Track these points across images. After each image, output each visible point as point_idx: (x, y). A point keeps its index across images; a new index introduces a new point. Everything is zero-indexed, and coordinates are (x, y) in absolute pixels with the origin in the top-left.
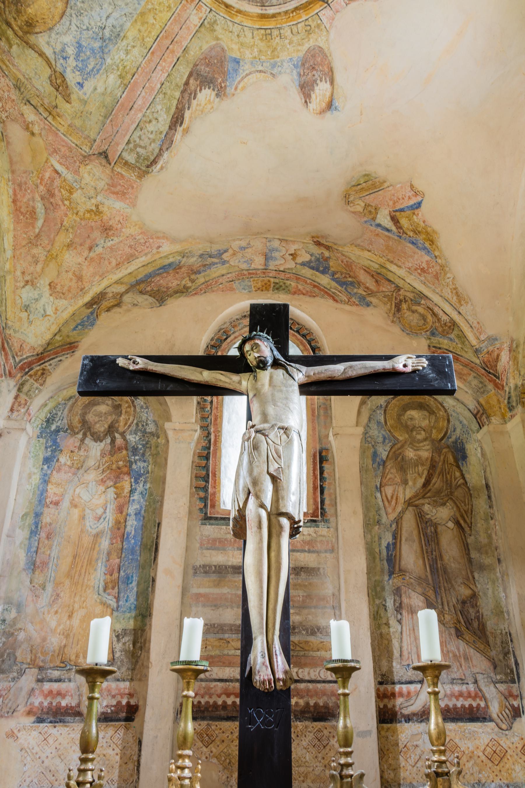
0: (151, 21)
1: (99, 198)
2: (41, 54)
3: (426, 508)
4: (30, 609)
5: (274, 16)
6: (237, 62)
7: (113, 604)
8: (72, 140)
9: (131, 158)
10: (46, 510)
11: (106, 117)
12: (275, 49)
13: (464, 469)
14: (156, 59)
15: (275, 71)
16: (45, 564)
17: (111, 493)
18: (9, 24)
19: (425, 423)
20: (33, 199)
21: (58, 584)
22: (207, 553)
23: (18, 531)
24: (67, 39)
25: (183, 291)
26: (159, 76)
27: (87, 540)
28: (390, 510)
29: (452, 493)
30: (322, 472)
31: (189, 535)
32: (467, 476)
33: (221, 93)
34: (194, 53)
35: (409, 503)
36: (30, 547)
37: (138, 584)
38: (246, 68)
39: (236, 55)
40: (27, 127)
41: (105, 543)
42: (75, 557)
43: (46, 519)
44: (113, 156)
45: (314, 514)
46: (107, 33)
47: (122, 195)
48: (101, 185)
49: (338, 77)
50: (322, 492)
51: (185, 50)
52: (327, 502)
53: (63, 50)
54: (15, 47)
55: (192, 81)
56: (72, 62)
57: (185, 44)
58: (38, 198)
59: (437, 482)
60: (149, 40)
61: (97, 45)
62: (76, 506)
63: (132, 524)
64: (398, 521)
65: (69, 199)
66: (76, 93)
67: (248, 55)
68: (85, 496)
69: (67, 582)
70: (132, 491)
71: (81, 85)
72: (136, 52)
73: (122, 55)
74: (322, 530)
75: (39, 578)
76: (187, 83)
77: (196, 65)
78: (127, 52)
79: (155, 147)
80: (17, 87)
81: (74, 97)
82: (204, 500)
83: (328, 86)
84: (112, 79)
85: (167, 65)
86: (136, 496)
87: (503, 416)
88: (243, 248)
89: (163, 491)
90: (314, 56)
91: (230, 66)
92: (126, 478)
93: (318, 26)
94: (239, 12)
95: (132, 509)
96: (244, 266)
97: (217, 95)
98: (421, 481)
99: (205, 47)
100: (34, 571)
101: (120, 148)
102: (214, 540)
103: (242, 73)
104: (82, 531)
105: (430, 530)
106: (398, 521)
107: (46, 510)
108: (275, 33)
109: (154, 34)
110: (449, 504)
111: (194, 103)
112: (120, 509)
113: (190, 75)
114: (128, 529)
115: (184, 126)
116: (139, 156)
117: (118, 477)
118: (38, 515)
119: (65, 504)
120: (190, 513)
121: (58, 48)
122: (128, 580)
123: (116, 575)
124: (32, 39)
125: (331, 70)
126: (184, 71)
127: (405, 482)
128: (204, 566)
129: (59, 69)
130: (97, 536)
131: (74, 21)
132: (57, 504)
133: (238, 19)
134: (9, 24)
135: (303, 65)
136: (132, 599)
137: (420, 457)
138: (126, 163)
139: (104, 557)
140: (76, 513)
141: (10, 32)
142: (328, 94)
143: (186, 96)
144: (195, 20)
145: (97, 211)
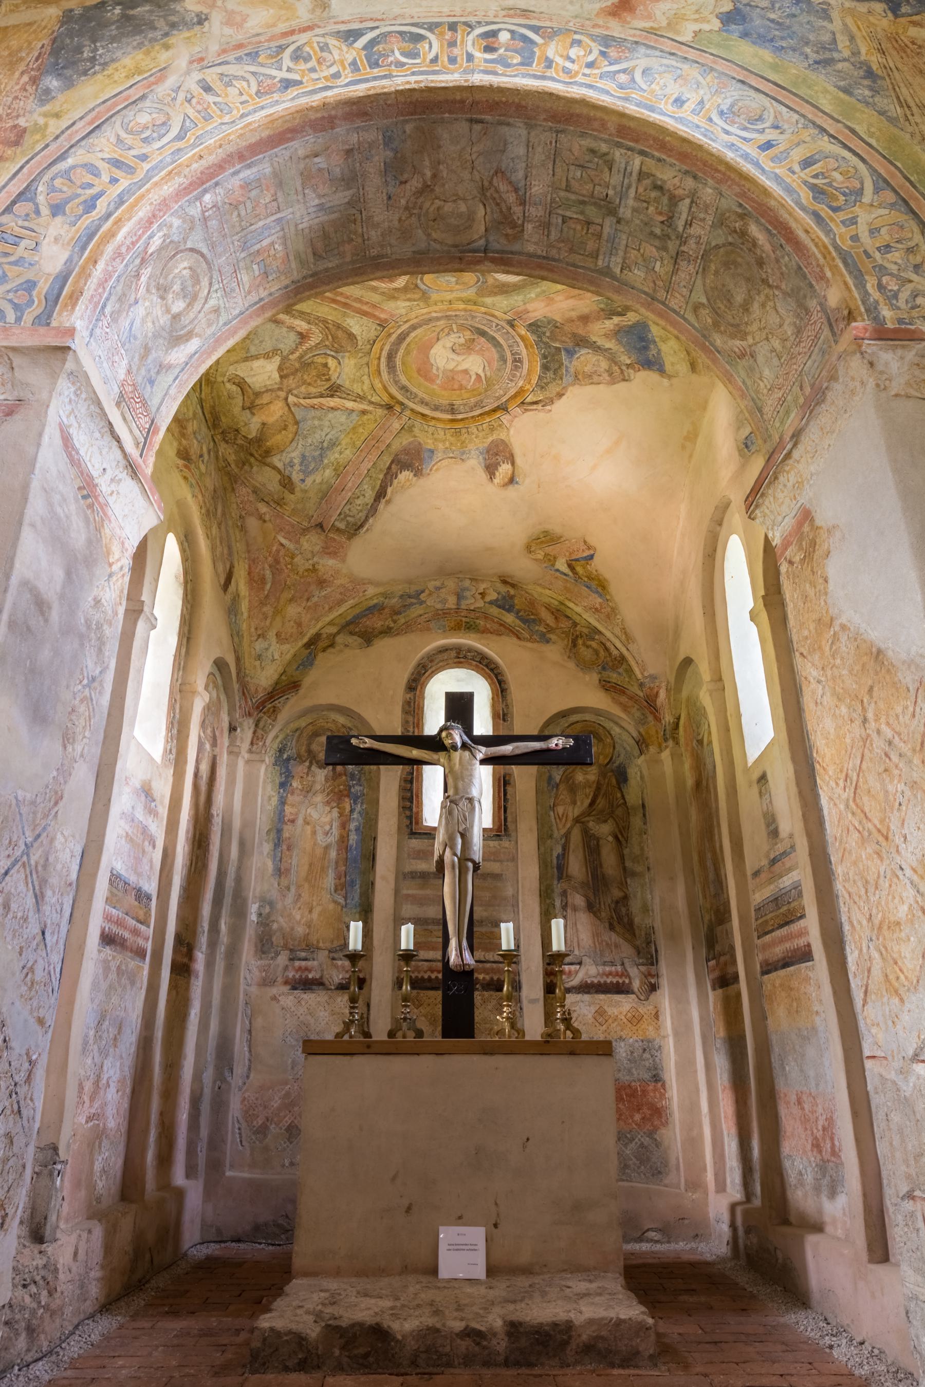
0: (361, 430)
1: (315, 559)
2: (275, 468)
3: (591, 824)
4: (279, 906)
5: (462, 420)
6: (432, 451)
7: (342, 901)
8: (294, 520)
9: (342, 525)
10: (285, 827)
11: (322, 499)
12: (463, 442)
13: (624, 791)
14: (364, 454)
15: (464, 457)
16: (288, 870)
18: (252, 455)
20: (264, 569)
21: (299, 887)
22: (413, 861)
23: (265, 844)
24: (293, 455)
26: (367, 465)
27: (319, 852)
28: (560, 826)
29: (613, 812)
30: (505, 794)
31: (399, 847)
32: (627, 797)
33: (418, 473)
34: (396, 446)
35: (577, 820)
36: (275, 856)
37: (361, 887)
38: (439, 455)
39: (431, 447)
40: (261, 518)
41: (333, 854)
42: (310, 865)
43: (286, 834)
45: (499, 830)
46: (325, 445)
47: (333, 554)
48: (317, 548)
49: (519, 460)
50: (505, 811)
51: (389, 446)
52: (509, 819)
53: (291, 461)
54: (255, 468)
55: (393, 466)
56: (297, 467)
57: (388, 442)
58: (267, 566)
59: (601, 803)
60: (358, 443)
61: (318, 453)
62: (308, 824)
63: (353, 838)
64: (567, 836)
65: (291, 564)
66: (299, 486)
67: (441, 446)
69: (306, 885)
71: (303, 481)
72: (348, 452)
73: (337, 455)
74: (505, 843)
75: (285, 882)
76: (389, 468)
77: (397, 455)
78: (341, 453)
80: (255, 492)
81: (297, 489)
83: (509, 466)
84: (328, 473)
85: (373, 457)
86: (355, 815)
87: (660, 745)
89: (377, 811)
90: (497, 446)
91: (426, 455)
92: (347, 800)
93: (500, 426)
94: (433, 418)
95: (353, 826)
97: (415, 475)
98: (587, 802)
99: (405, 442)
100: (280, 876)
101: (333, 519)
102: (419, 852)
103: (435, 459)
104: (315, 844)
105: (594, 842)
106: (567, 836)
107: (285, 827)
108: (464, 431)
109: (363, 438)
110: (610, 821)
111: (395, 482)
112: (343, 826)
113: (392, 462)
114: (351, 842)
115: (387, 498)
116: (348, 523)
117: (340, 799)
118: (279, 831)
119: (300, 821)
120: (399, 828)
121: (288, 460)
122: (352, 884)
123: (343, 880)
124: (268, 460)
125: (512, 456)
126: (387, 460)
127: (574, 803)
128: (411, 873)
129: (287, 473)
130: (327, 848)
131: (301, 442)
132: (293, 821)
133: (433, 423)
134: (252, 455)
135: (488, 452)
136: (357, 898)
137: (588, 781)
138: (338, 530)
139: (333, 864)
140: (308, 829)
141: (252, 460)
142: (510, 472)
143: (389, 477)
144: (397, 425)
145: (314, 570)
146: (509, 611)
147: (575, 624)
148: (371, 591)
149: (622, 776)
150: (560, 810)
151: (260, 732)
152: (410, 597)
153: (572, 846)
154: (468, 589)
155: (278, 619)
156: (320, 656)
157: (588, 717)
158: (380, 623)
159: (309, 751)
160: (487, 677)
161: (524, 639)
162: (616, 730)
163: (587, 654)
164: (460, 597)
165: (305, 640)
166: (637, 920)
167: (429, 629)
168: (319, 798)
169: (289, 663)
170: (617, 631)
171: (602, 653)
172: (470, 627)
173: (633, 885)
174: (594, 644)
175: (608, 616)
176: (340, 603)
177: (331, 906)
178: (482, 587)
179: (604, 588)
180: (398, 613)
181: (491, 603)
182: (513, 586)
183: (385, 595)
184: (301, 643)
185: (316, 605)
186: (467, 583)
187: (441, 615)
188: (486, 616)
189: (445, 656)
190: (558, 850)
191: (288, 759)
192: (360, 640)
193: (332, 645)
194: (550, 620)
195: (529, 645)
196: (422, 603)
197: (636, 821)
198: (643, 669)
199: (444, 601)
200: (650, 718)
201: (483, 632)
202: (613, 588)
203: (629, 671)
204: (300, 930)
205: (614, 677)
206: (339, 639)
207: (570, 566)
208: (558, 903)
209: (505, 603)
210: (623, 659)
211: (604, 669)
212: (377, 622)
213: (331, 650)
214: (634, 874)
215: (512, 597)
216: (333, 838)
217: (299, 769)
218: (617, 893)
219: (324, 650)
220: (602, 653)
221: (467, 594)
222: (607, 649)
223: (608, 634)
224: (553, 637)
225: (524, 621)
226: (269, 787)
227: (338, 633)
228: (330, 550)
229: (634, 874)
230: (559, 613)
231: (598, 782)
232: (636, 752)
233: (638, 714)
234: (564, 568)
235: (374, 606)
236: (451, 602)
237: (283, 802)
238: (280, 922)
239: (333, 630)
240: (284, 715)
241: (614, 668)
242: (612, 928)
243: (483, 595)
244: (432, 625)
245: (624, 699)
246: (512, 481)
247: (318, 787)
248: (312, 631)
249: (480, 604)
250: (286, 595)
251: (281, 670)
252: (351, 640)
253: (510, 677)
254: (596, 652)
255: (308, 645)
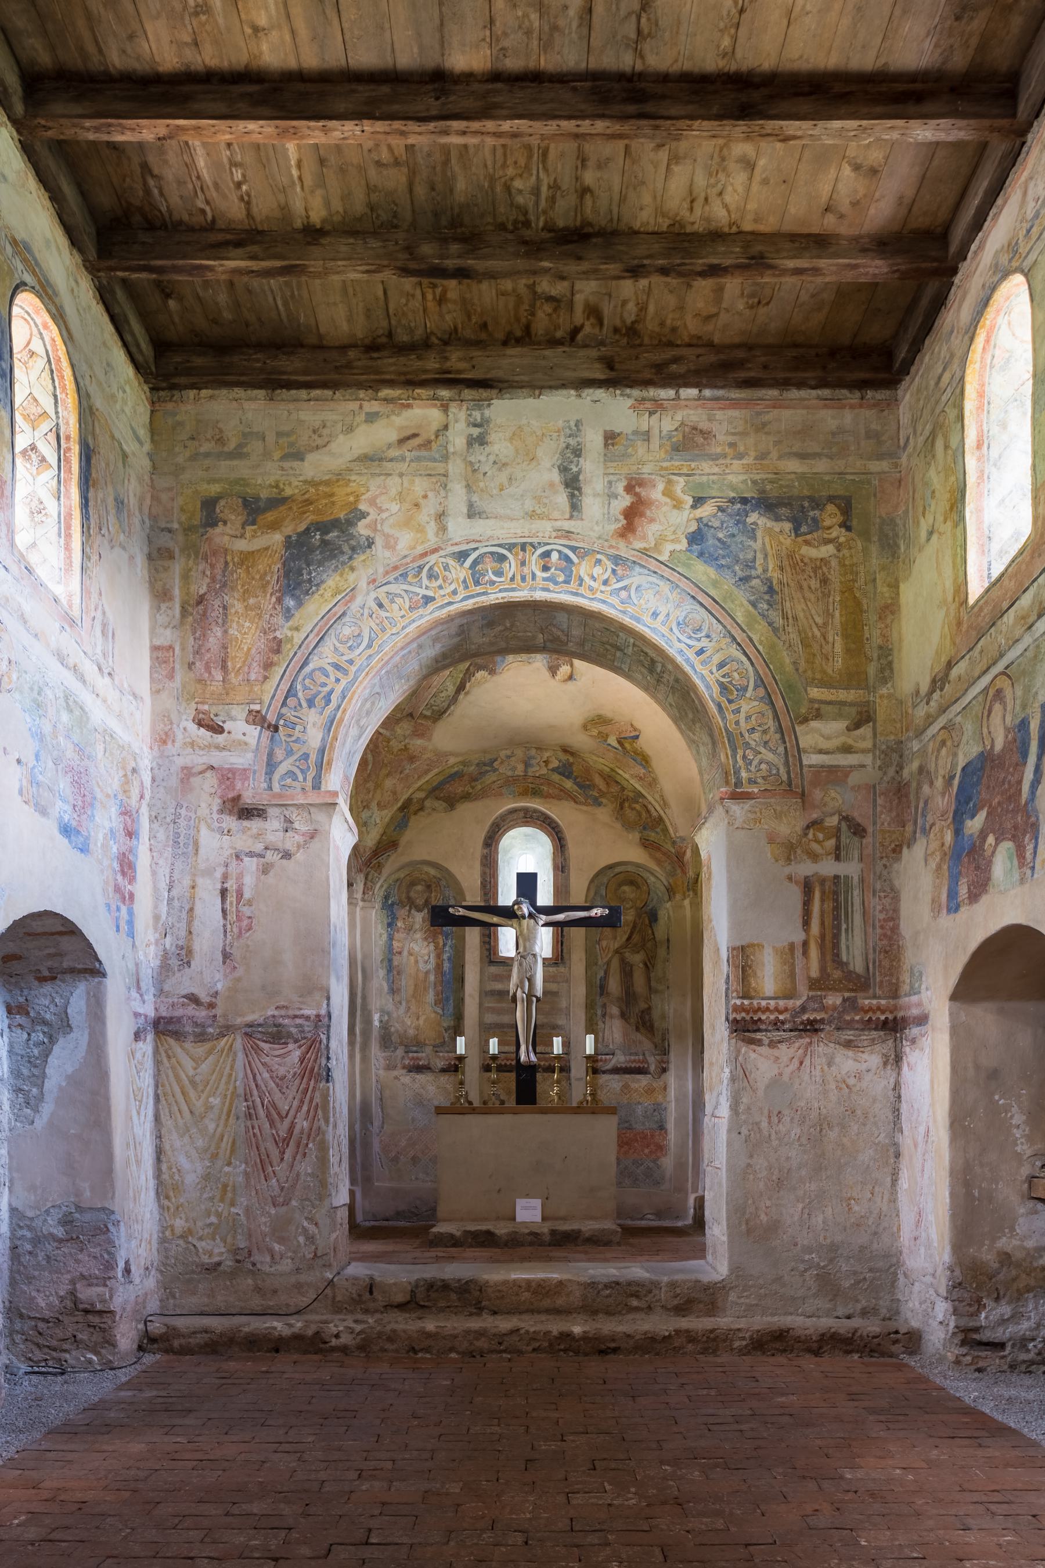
3: (627, 955)
4: (395, 1015)
9: (428, 713)
16: (399, 990)
17: (432, 947)
19: (632, 896)
21: (408, 1002)
25: (466, 797)
27: (421, 976)
31: (482, 972)
35: (617, 951)
41: (432, 978)
43: (395, 963)
44: (417, 714)
47: (421, 736)
48: (408, 732)
59: (636, 938)
63: (446, 966)
64: (608, 963)
68: (417, 949)
70: (445, 945)
74: (562, 969)
75: (397, 998)
79: (445, 704)
82: (489, 950)
88: (508, 757)
95: (445, 956)
96: (510, 773)
105: (628, 969)
106: (608, 963)
110: (642, 952)
112: (439, 956)
118: (390, 961)
119: (405, 953)
122: (447, 999)
127: (615, 938)
130: (427, 973)
138: (426, 717)
140: (412, 958)
146: (568, 777)
147: (623, 789)
148: (452, 760)
149: (653, 917)
150: (604, 943)
151: (369, 884)
152: (485, 765)
153: (612, 971)
154: (534, 758)
155: (379, 791)
156: (413, 818)
157: (629, 868)
158: (461, 789)
159: (409, 898)
160: (549, 835)
161: (581, 803)
162: (652, 879)
163: (630, 815)
164: (527, 765)
165: (400, 804)
166: (656, 1024)
167: (501, 795)
168: (418, 936)
169: (388, 825)
170: (657, 797)
171: (644, 814)
172: (535, 793)
173: (655, 999)
174: (638, 807)
175: (650, 784)
176: (426, 772)
177: (433, 1015)
178: (546, 755)
179: (647, 762)
180: (476, 780)
181: (553, 770)
182: (572, 754)
183: (464, 763)
184: (396, 808)
185: (408, 776)
186: (533, 752)
187: (510, 781)
188: (549, 783)
189: (515, 816)
190: (602, 974)
191: (393, 904)
192: (444, 805)
193: (422, 809)
194: (601, 784)
195: (584, 808)
196: (495, 770)
197: (662, 952)
198: (676, 831)
199: (514, 769)
200: (679, 871)
201: (546, 797)
202: (654, 763)
203: (665, 830)
204: (411, 1032)
205: (652, 835)
206: (428, 803)
207: (619, 742)
208: (599, 1012)
209: (565, 771)
210: (660, 820)
211: (644, 828)
212: (459, 788)
213: (421, 813)
214: (656, 991)
215: (571, 765)
216: (432, 965)
217: (402, 912)
218: (643, 1006)
219: (415, 813)
220: (644, 814)
221: (533, 762)
222: (648, 811)
223: (650, 798)
224: (604, 801)
225: (580, 786)
226: (379, 926)
227: (426, 798)
228: (418, 733)
229: (656, 991)
230: (610, 778)
231: (635, 923)
232: (666, 897)
233: (669, 868)
234: (615, 744)
235: (456, 773)
236: (520, 769)
237: (391, 938)
238: (396, 1027)
239: (421, 795)
240: (386, 871)
241: (653, 829)
242: (637, 1029)
243: (546, 762)
244: (504, 790)
245: (659, 855)
246: (571, 677)
247: (417, 926)
248: (405, 797)
249: (544, 771)
250: (384, 772)
251: (381, 831)
252: (437, 804)
253: (569, 835)
254: (639, 814)
255: (402, 808)
